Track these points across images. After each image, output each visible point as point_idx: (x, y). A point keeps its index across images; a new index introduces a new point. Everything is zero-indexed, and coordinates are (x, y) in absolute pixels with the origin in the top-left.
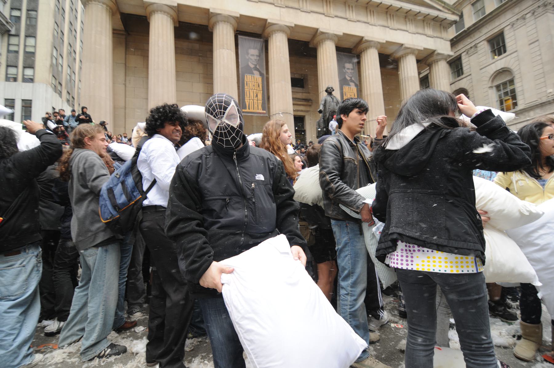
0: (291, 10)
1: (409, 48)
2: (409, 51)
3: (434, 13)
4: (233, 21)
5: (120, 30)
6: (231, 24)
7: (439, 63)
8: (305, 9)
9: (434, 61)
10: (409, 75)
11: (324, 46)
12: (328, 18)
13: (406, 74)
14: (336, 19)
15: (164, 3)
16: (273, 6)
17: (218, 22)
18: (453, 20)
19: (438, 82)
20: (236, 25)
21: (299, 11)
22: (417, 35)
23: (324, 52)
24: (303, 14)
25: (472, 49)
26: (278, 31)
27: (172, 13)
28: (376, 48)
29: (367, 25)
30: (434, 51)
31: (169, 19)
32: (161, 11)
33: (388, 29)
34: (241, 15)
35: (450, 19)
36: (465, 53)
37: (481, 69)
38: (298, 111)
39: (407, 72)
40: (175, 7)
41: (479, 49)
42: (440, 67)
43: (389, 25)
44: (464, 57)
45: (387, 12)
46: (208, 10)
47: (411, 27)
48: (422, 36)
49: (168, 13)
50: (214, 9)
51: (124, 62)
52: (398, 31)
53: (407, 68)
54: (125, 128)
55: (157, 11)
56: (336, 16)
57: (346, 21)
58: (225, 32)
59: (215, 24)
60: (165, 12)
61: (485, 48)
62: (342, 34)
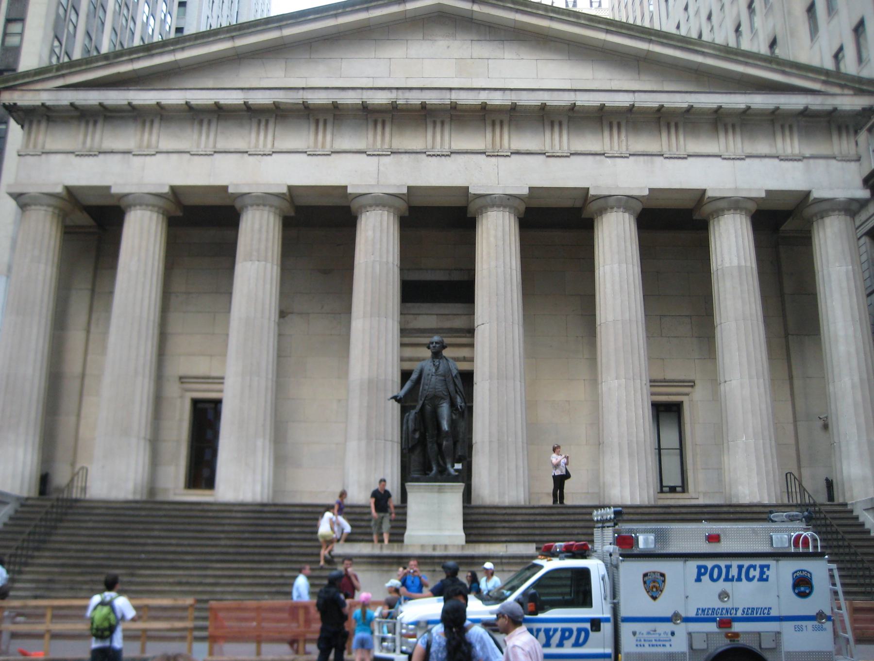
0: (405, 157)
1: (724, 198)
4: (277, 202)
5: (90, 227)
6: (271, 206)
7: (828, 221)
8: (438, 149)
9: (815, 215)
10: (727, 264)
11: (484, 221)
12: (494, 159)
13: (719, 263)
14: (514, 157)
15: (146, 191)
16: (364, 156)
17: (246, 207)
18: (859, 108)
19: (825, 272)
20: (285, 205)
21: (424, 156)
22: (748, 160)
23: (485, 235)
24: (434, 159)
26: (371, 206)
27: (161, 202)
28: (627, 209)
29: (598, 158)
30: (808, 193)
31: (155, 216)
32: (141, 205)
34: (290, 188)
35: (848, 108)
38: (465, 359)
39: (722, 255)
40: (166, 194)
42: (829, 231)
43: (665, 149)
45: (660, 118)
46: (225, 188)
47: (734, 144)
48: (767, 160)
49: (154, 206)
50: (237, 185)
51: (89, 287)
52: (690, 159)
53: (721, 247)
54: (79, 415)
55: (135, 205)
56: (518, 153)
57: (542, 157)
58: (257, 226)
59: (244, 207)
60: (147, 205)
62: (525, 191)
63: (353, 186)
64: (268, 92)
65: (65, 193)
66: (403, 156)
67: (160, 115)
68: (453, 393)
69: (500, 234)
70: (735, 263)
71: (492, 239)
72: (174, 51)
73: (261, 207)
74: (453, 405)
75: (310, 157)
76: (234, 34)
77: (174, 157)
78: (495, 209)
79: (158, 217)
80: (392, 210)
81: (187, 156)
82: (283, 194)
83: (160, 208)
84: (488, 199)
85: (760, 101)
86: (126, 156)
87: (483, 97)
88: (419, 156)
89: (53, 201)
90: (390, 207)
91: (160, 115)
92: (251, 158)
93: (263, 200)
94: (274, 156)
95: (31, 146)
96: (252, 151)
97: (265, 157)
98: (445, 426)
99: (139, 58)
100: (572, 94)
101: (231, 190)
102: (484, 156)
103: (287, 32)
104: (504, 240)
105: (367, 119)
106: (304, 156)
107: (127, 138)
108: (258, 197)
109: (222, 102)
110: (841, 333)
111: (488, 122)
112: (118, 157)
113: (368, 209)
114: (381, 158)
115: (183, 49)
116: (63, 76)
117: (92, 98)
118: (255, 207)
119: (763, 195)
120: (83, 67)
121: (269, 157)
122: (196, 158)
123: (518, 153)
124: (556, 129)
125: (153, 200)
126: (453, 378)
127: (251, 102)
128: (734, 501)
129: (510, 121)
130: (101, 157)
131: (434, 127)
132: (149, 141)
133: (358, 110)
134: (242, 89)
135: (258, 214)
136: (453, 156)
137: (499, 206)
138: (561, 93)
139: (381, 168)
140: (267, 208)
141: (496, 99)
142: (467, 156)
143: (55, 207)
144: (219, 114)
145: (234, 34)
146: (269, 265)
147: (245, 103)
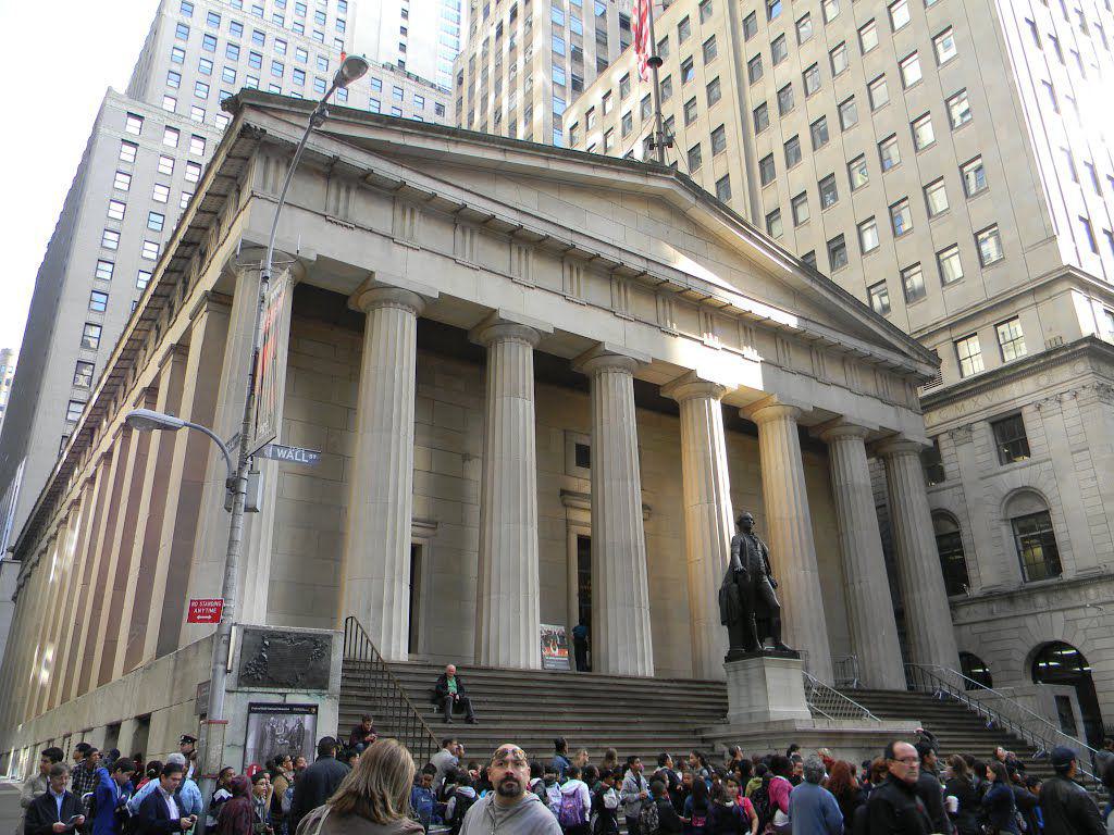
0: (645, 327)
2: (854, 430)
3: (897, 360)
17: (509, 336)
25: (961, 434)
32: (402, 304)
33: (814, 381)
36: (945, 436)
37: (982, 479)
41: (974, 435)
42: (908, 467)
44: (946, 445)
61: (984, 436)
67: (427, 206)
70: (862, 481)
72: (448, 141)
75: (567, 303)
76: (507, 148)
77: (438, 259)
85: (879, 352)
86: (387, 241)
91: (427, 206)
92: (515, 286)
94: (536, 291)
95: (269, 190)
96: (517, 279)
103: (555, 166)
105: (611, 279)
107: (379, 215)
110: (924, 552)
112: (377, 240)
119: (878, 429)
120: (351, 120)
122: (460, 267)
128: (878, 687)
130: (357, 232)
133: (606, 267)
144: (486, 227)
145: (507, 148)
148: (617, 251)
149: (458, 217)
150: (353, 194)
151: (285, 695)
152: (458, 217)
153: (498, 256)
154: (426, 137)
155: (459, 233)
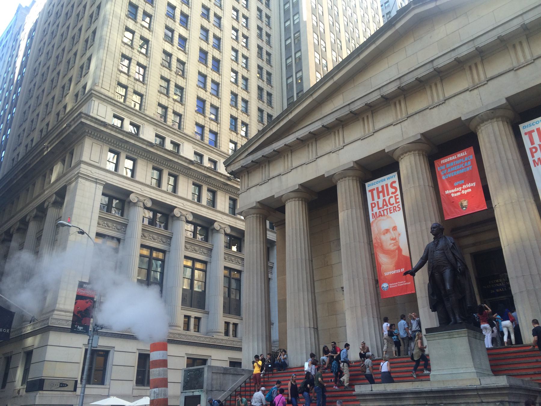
0: (416, 117)
4: (351, 173)
6: (349, 176)
12: (476, 91)
14: (490, 83)
16: (392, 127)
21: (428, 110)
24: (435, 109)
26: (402, 154)
49: (295, 198)
57: (512, 74)
58: (343, 190)
60: (292, 198)
62: (504, 101)
63: (388, 147)
64: (332, 115)
65: (258, 205)
66: (415, 116)
67: (290, 149)
68: (453, 261)
69: (493, 139)
71: (488, 145)
72: (287, 115)
73: (344, 179)
74: (454, 270)
77: (299, 168)
78: (486, 123)
79: (299, 203)
80: (417, 152)
81: (304, 166)
82: (352, 167)
83: (299, 198)
84: (477, 117)
87: (454, 55)
88: (424, 112)
89: (253, 211)
90: (415, 151)
92: (334, 154)
93: (344, 174)
94: (345, 148)
97: (340, 151)
98: (448, 287)
99: (274, 127)
100: (520, 18)
101: (326, 176)
102: (468, 92)
103: (336, 78)
104: (497, 141)
106: (359, 142)
108: (339, 174)
109: (312, 131)
111: (467, 68)
112: (277, 178)
113: (402, 157)
114: (402, 123)
115: (291, 112)
116: (247, 149)
117: (258, 155)
118: (341, 180)
121: (342, 150)
123: (492, 79)
124: (518, 48)
125: (293, 195)
126: (450, 249)
127: (325, 124)
129: (482, 60)
130: (270, 181)
131: (432, 90)
132: (288, 165)
134: (320, 119)
135: (343, 183)
136: (447, 101)
137: (487, 120)
138: (511, 22)
139: (403, 130)
140: (347, 178)
141: (464, 51)
142: (456, 98)
143: (257, 214)
146: (354, 211)
147: (323, 126)
148: (378, 91)
149: (303, 143)
150: (267, 167)
151: (193, 392)
152: (303, 143)
153: (326, 145)
154: (279, 122)
155: (307, 149)
